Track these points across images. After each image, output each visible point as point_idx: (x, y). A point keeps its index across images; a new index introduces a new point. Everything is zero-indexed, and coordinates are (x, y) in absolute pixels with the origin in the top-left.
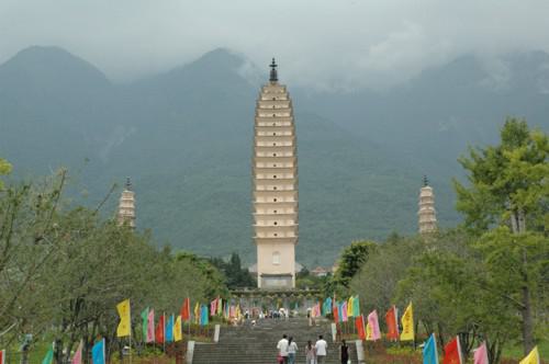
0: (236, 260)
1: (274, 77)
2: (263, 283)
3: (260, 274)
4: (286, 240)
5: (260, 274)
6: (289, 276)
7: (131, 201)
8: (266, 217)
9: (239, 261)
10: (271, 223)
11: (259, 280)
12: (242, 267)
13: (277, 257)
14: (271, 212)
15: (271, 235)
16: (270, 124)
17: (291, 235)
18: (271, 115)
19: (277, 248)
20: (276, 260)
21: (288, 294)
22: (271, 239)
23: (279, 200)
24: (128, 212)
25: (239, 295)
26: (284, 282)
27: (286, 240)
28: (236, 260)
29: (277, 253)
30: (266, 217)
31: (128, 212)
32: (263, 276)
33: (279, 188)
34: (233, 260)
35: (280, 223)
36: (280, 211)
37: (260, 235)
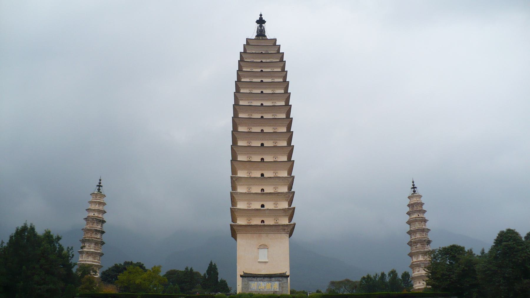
1: (261, 33)
2: (245, 286)
4: (277, 228)
5: (240, 272)
6: (283, 276)
7: (100, 203)
10: (256, 205)
11: (239, 281)
14: (256, 189)
15: (256, 221)
16: (259, 80)
17: (285, 221)
18: (259, 70)
19: (265, 239)
20: (263, 255)
22: (256, 226)
24: (96, 214)
26: (274, 287)
29: (264, 246)
31: (96, 214)
32: (245, 276)
33: (267, 159)
35: (269, 205)
36: (269, 189)
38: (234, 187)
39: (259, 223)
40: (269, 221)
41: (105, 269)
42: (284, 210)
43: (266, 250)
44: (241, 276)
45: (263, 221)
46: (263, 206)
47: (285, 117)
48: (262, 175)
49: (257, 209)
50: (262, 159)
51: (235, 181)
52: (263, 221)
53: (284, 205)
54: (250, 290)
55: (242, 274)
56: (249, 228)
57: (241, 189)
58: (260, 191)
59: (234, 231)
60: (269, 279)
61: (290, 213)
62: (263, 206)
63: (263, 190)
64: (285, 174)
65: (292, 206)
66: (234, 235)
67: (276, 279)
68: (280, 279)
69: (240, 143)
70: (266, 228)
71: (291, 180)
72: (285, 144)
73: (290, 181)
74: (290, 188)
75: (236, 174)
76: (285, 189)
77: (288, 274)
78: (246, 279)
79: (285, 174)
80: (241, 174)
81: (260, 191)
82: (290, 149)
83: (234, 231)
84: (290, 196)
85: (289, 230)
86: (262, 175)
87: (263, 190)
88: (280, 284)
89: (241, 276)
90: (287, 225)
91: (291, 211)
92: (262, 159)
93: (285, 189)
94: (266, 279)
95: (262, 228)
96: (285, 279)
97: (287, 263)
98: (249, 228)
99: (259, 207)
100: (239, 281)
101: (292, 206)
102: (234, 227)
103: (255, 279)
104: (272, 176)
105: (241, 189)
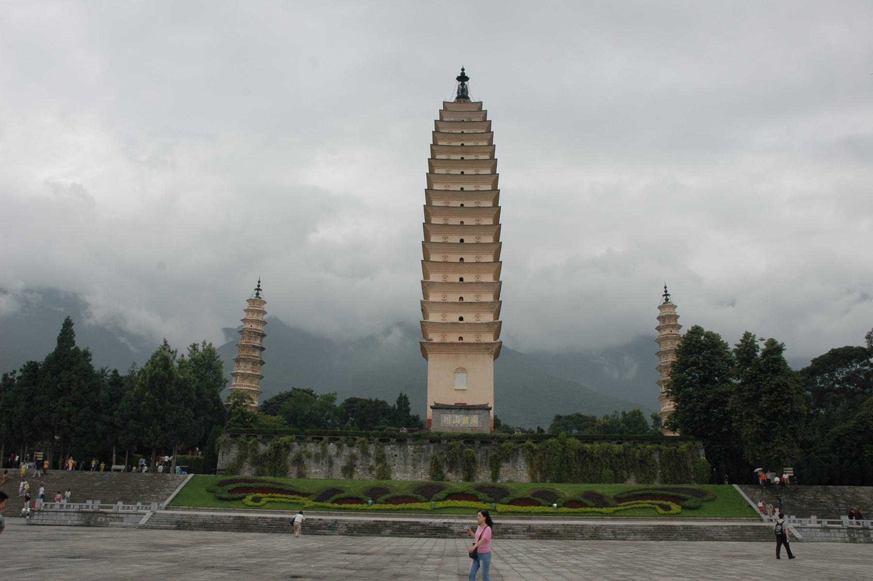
0: (403, 401)
3: (430, 403)
4: (478, 347)
5: (430, 403)
6: (485, 408)
8: (444, 305)
9: (407, 403)
10: (453, 318)
11: (430, 411)
12: (411, 413)
13: (462, 376)
14: (454, 298)
15: (453, 338)
17: (489, 338)
19: (463, 361)
20: (460, 382)
21: (484, 440)
23: (468, 278)
25: (385, 440)
27: (478, 347)
28: (403, 401)
29: (462, 370)
30: (444, 305)
32: (437, 407)
34: (399, 402)
35: (469, 318)
36: (469, 298)
37: (436, 338)
38: (425, 295)
39: (456, 340)
40: (469, 338)
41: (268, 397)
42: (488, 324)
43: (465, 375)
44: (432, 407)
45: (461, 338)
46: (461, 319)
47: (491, 205)
48: (461, 279)
49: (454, 324)
50: (462, 259)
51: (426, 286)
52: (461, 338)
53: (488, 318)
54: (442, 425)
55: (433, 404)
56: (444, 346)
57: (434, 297)
58: (457, 300)
59: (425, 349)
60: (466, 412)
61: (496, 328)
62: (461, 319)
63: (461, 298)
64: (489, 278)
65: (500, 319)
66: (425, 356)
67: (476, 411)
68: (481, 411)
69: (433, 239)
70: (465, 347)
71: (497, 286)
72: (490, 240)
73: (496, 287)
74: (497, 296)
75: (429, 278)
76: (489, 298)
77: (489, 406)
78: (436, 411)
79: (489, 278)
80: (434, 278)
81: (457, 300)
82: (497, 246)
83: (425, 349)
84: (496, 307)
85: (494, 350)
86: (461, 279)
87: (461, 298)
88: (479, 418)
89: (432, 407)
90: (491, 343)
91: (496, 326)
92: (462, 259)
93: (489, 298)
94: (462, 411)
95: (460, 347)
96: (486, 412)
97: (491, 393)
98: (444, 346)
99: (457, 320)
100: (430, 411)
101: (500, 319)
102: (426, 346)
103: (448, 411)
104: (474, 281)
105: (434, 297)
